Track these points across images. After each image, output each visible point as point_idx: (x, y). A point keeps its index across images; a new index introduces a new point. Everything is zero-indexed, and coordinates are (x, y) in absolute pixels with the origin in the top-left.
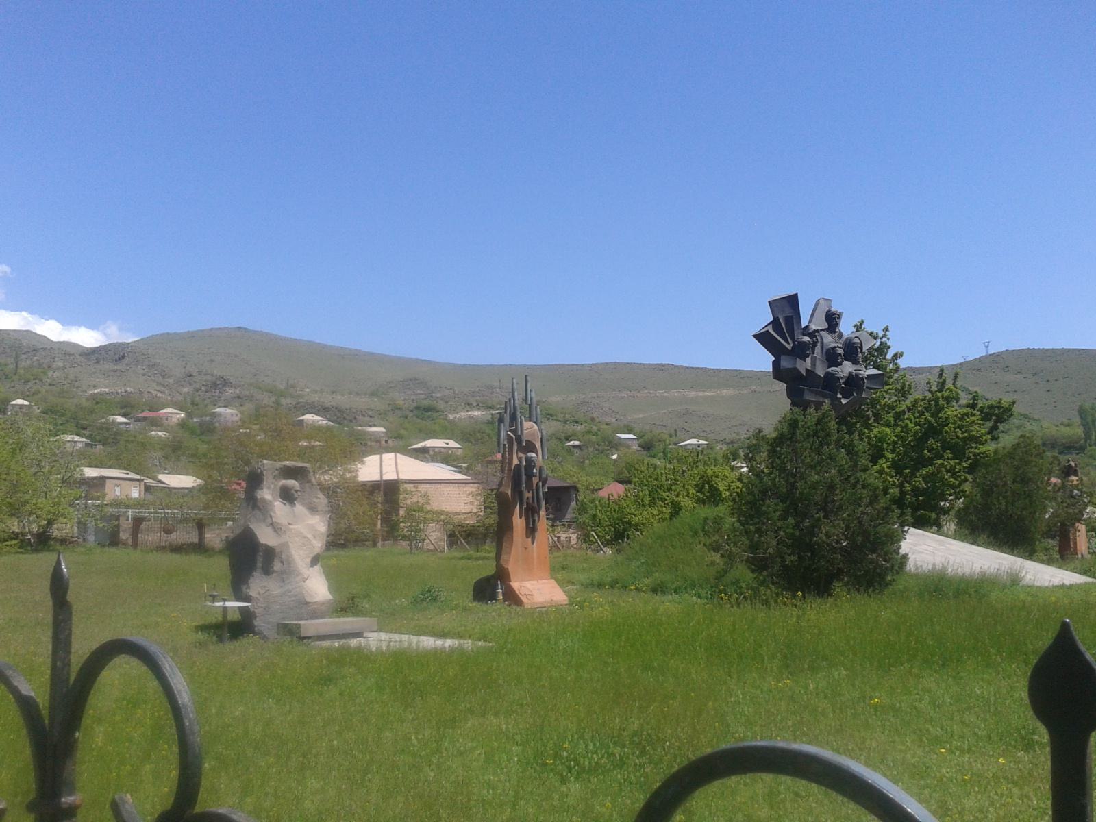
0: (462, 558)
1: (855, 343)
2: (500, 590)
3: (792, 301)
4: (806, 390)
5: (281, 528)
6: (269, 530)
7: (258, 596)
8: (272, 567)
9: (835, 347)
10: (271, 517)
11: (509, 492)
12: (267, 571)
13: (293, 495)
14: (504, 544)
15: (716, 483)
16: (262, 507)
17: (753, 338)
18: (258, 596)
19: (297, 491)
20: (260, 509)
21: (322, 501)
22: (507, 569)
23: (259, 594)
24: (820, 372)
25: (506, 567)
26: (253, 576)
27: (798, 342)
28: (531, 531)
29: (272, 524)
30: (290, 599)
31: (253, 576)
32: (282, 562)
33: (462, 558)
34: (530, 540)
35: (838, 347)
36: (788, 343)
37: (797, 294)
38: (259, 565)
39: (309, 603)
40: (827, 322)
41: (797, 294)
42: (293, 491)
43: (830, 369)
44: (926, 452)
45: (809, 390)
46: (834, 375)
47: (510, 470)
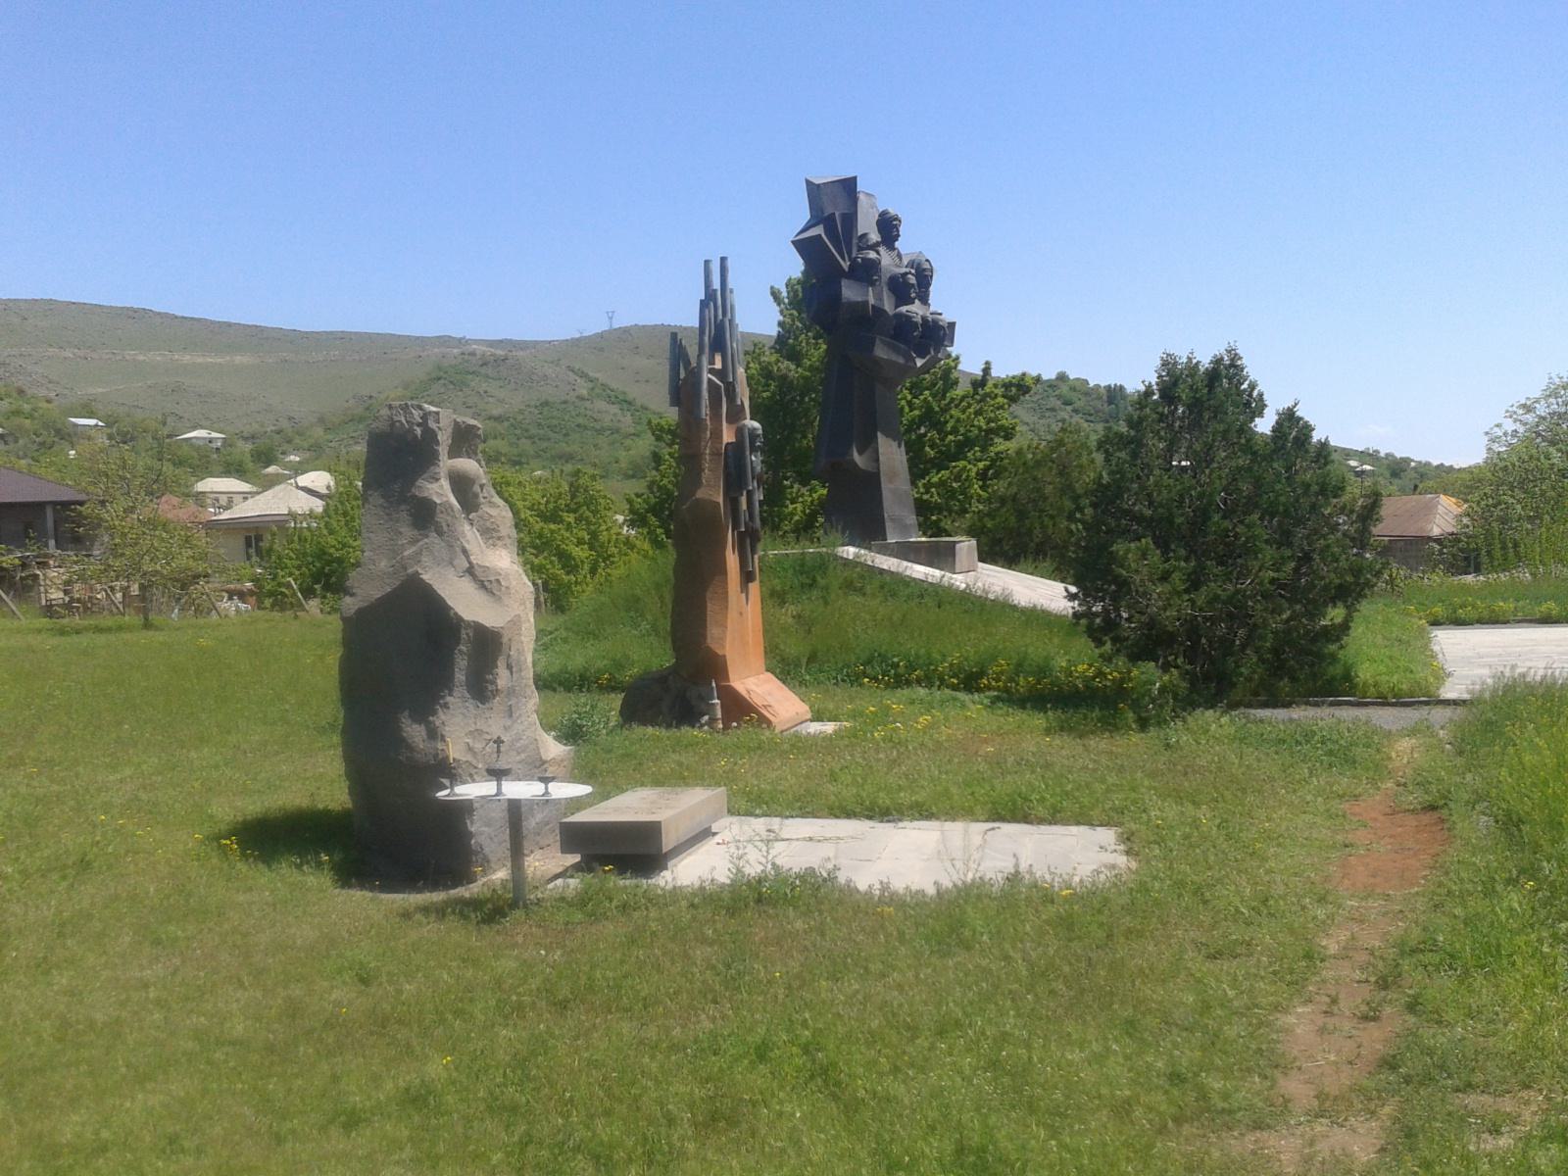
0: (39, 631)
1: (925, 270)
2: (717, 701)
3: (849, 186)
4: (878, 342)
5: (498, 581)
6: (466, 585)
7: (469, 757)
8: (493, 682)
9: (907, 274)
10: (465, 552)
11: (721, 500)
12: (481, 690)
13: (476, 496)
14: (709, 605)
15: (510, 495)
16: (445, 528)
17: (792, 246)
18: (469, 757)
19: (482, 486)
20: (440, 533)
21: (504, 513)
22: (724, 656)
23: (470, 749)
24: (888, 306)
25: (720, 652)
26: (446, 706)
27: (862, 259)
28: (747, 577)
29: (471, 571)
30: (518, 758)
31: (446, 706)
32: (509, 667)
33: (39, 631)
34: (744, 595)
35: (910, 273)
36: (844, 259)
37: (855, 178)
38: (460, 676)
39: (544, 762)
40: (880, 231)
41: (855, 178)
42: (476, 488)
43: (904, 309)
44: (927, 449)
45: (883, 342)
46: (911, 317)
47: (715, 454)
